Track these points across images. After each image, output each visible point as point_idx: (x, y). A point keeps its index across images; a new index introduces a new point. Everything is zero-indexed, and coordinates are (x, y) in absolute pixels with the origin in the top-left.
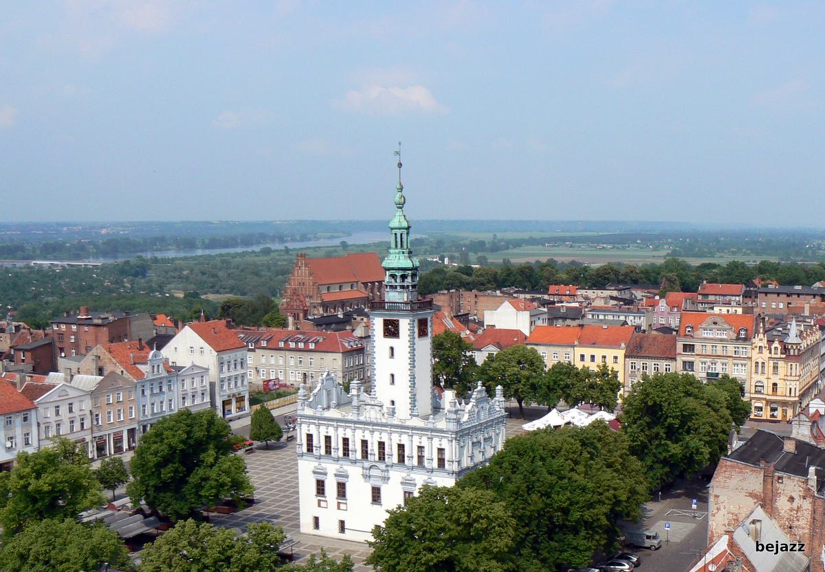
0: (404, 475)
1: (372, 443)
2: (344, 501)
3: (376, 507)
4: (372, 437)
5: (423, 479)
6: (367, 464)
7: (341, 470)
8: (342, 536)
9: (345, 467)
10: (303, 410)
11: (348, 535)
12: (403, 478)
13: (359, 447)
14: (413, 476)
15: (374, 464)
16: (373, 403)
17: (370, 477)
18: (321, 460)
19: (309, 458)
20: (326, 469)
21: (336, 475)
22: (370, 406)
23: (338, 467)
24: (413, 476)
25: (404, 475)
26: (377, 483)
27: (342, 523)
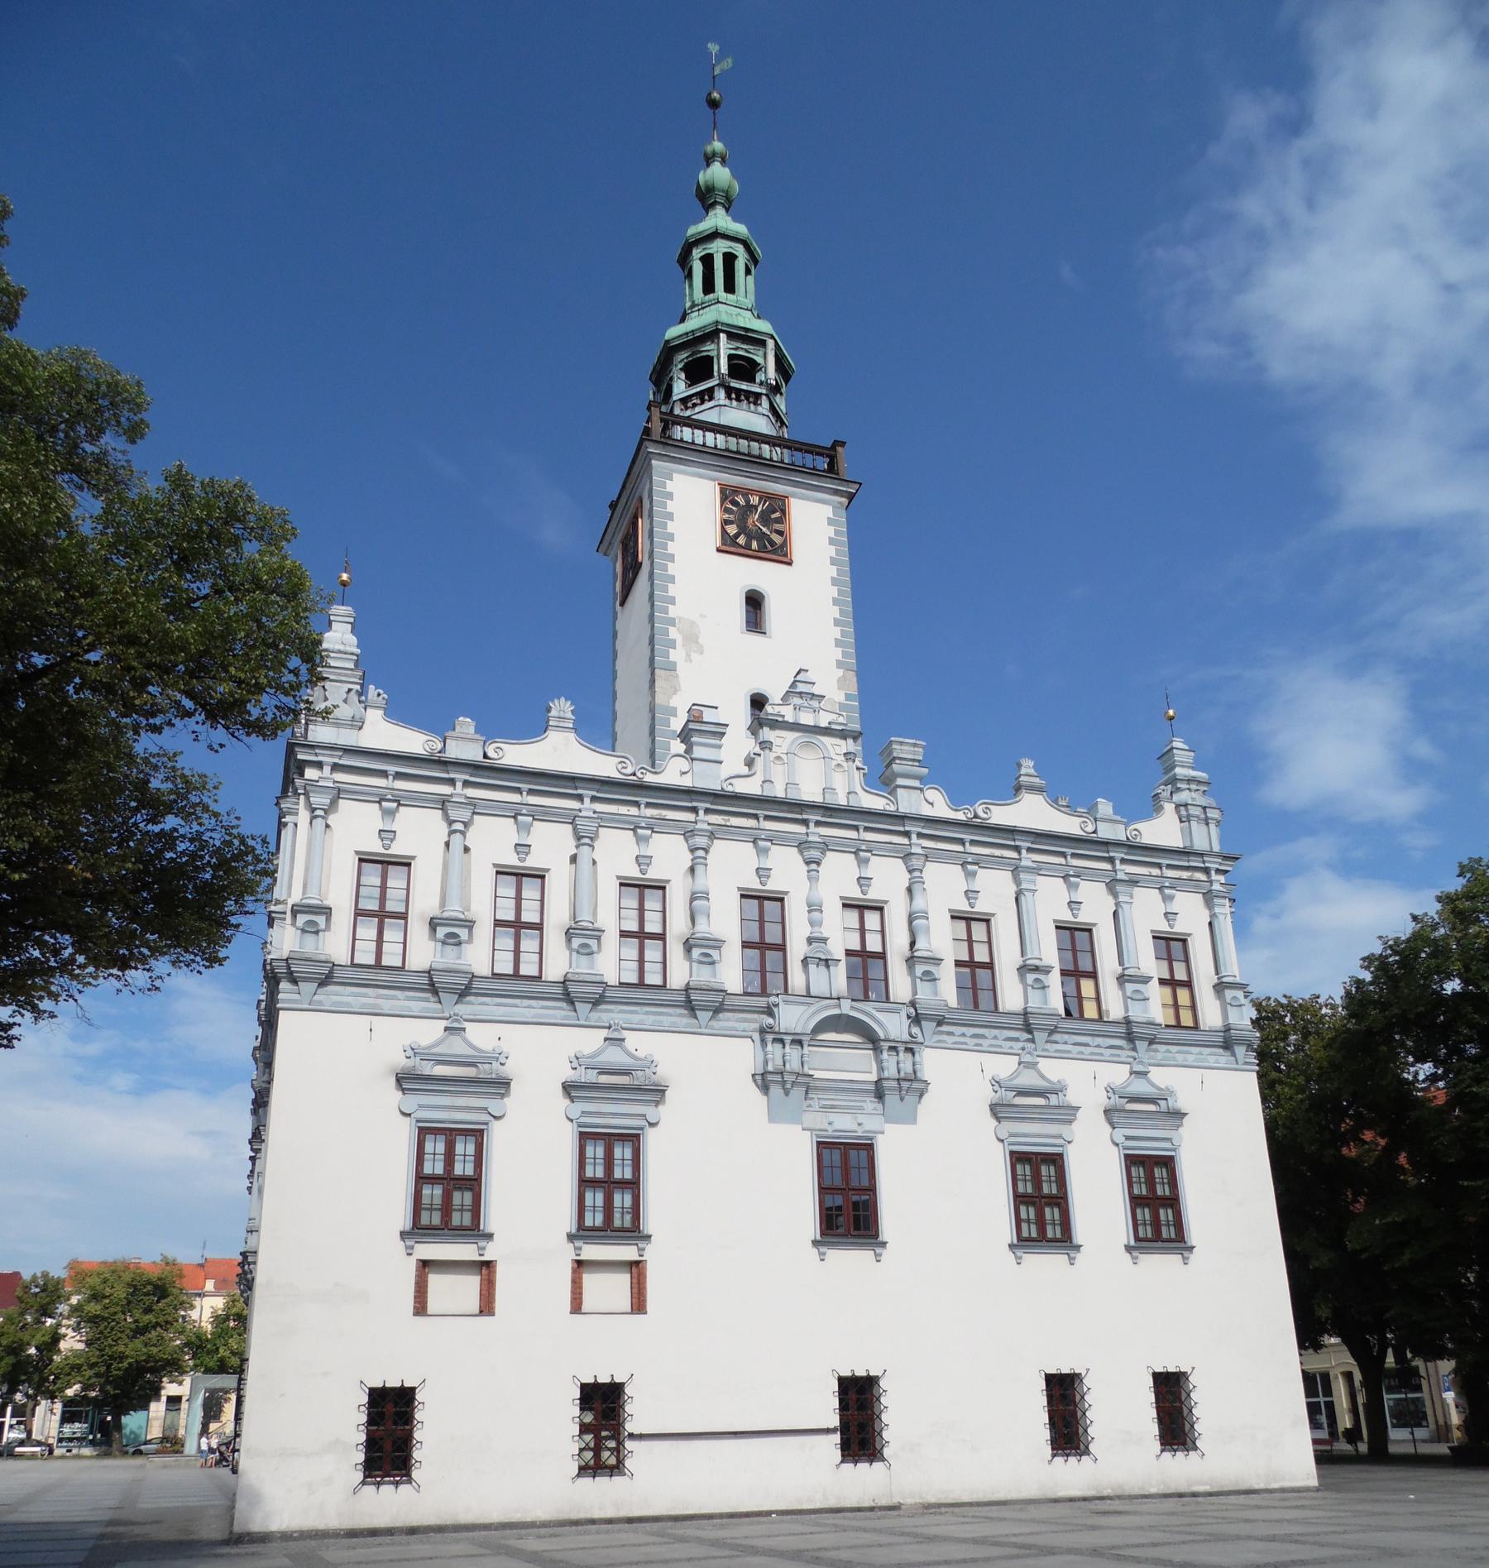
0: (1004, 1066)
1: (814, 907)
2: (627, 1253)
3: (849, 1259)
4: (813, 877)
5: (1102, 1083)
6: (792, 1017)
7: (614, 1057)
8: (603, 1497)
9: (633, 1040)
10: (358, 724)
11: (654, 1481)
12: (996, 1083)
13: (726, 921)
14: (1053, 1070)
15: (846, 1008)
16: (807, 719)
17: (807, 1085)
18: (471, 1007)
19: (369, 997)
20: (498, 1057)
21: (570, 1089)
22: (791, 736)
23: (589, 1041)
24: (1053, 1070)
25: (1004, 1066)
26: (844, 1125)
27: (602, 1404)
